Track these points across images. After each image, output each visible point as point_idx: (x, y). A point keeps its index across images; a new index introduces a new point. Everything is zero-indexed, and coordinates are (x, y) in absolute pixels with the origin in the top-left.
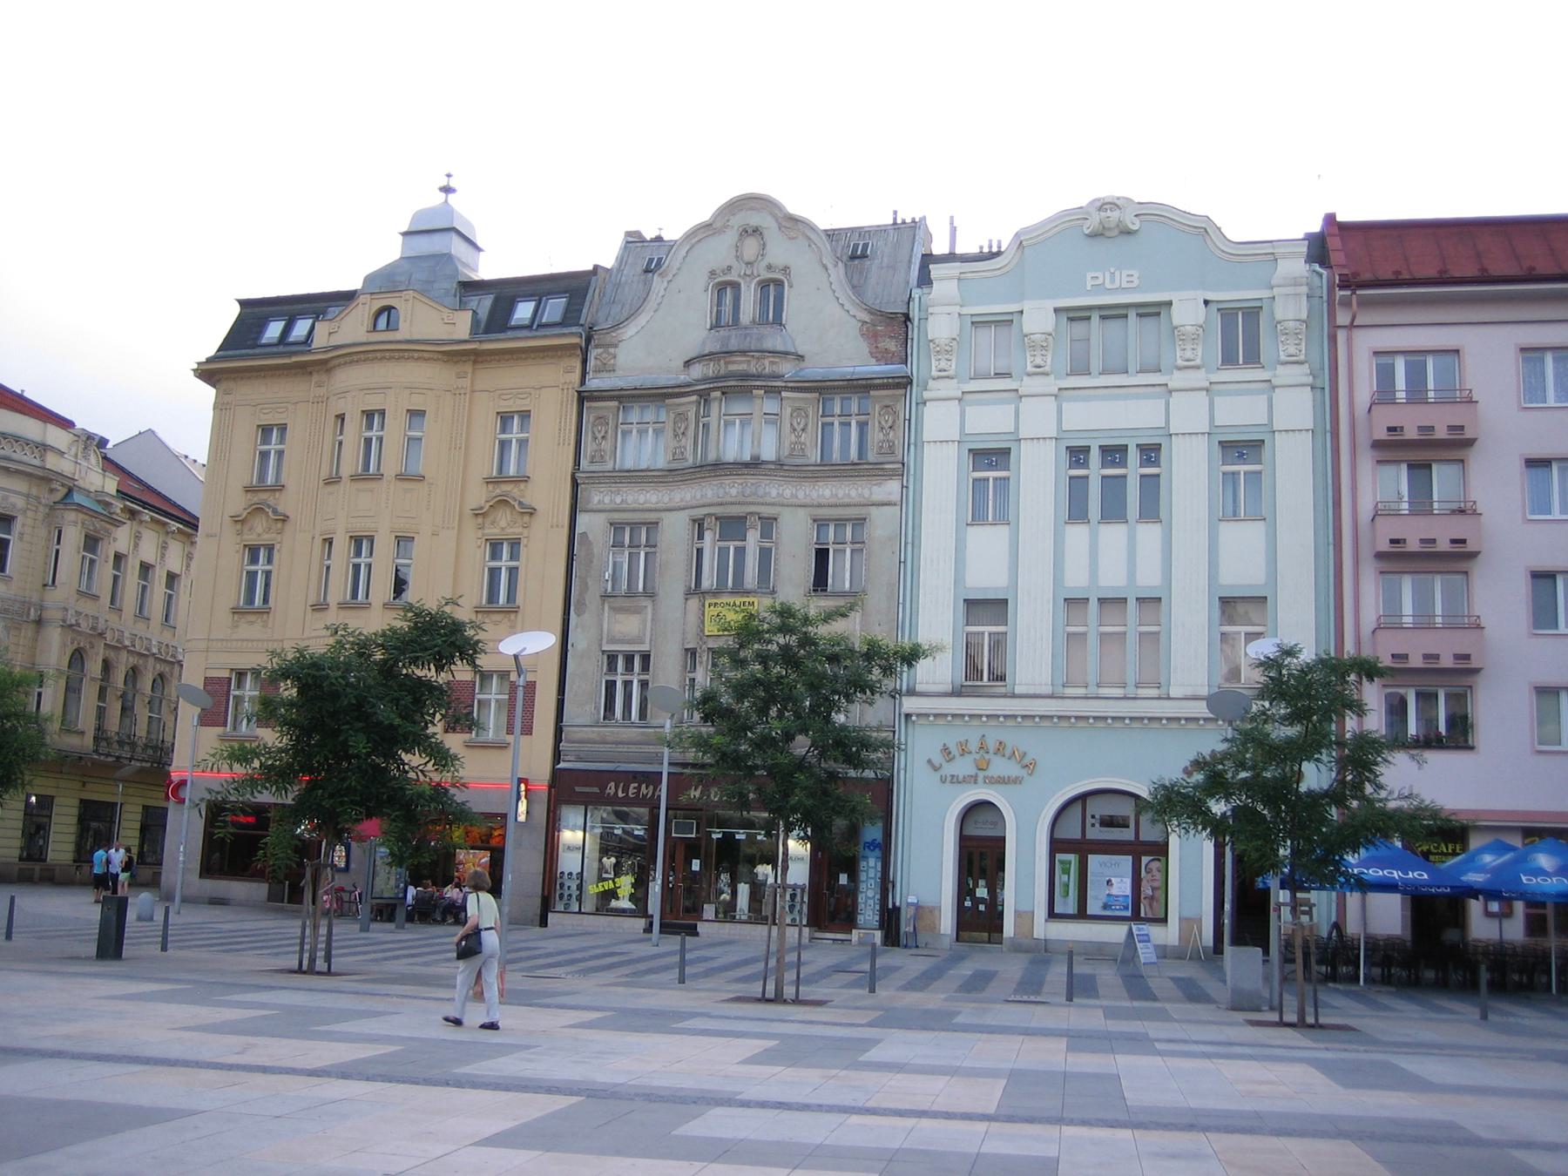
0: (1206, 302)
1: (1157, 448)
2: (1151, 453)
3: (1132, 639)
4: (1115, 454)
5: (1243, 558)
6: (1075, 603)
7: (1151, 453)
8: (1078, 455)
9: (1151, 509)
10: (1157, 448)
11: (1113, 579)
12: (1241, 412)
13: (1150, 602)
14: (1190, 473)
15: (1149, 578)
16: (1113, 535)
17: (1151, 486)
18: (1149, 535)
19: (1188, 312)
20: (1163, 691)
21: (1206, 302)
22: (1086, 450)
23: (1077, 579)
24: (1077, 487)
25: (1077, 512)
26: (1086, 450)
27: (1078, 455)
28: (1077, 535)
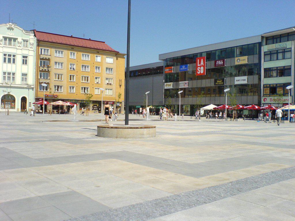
0: (22, 39)
1: (15, 56)
2: (14, 56)
3: (11, 78)
4: (10, 55)
5: (25, 69)
6: (5, 73)
7: (14, 56)
8: (5, 55)
9: (14, 62)
10: (15, 56)
11: (9, 70)
12: (25, 52)
13: (14, 74)
14: (19, 59)
15: (14, 71)
16: (9, 65)
17: (14, 60)
18: (14, 65)
19: (20, 40)
20: (15, 84)
21: (22, 39)
22: (6, 55)
23: (5, 70)
24: (5, 59)
25: (5, 61)
26: (6, 55)
27: (5, 55)
28: (5, 65)
